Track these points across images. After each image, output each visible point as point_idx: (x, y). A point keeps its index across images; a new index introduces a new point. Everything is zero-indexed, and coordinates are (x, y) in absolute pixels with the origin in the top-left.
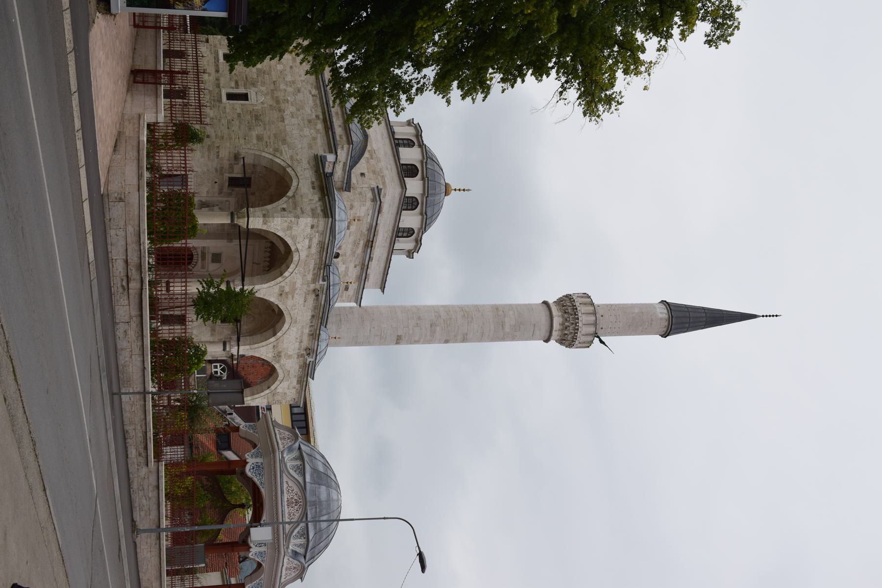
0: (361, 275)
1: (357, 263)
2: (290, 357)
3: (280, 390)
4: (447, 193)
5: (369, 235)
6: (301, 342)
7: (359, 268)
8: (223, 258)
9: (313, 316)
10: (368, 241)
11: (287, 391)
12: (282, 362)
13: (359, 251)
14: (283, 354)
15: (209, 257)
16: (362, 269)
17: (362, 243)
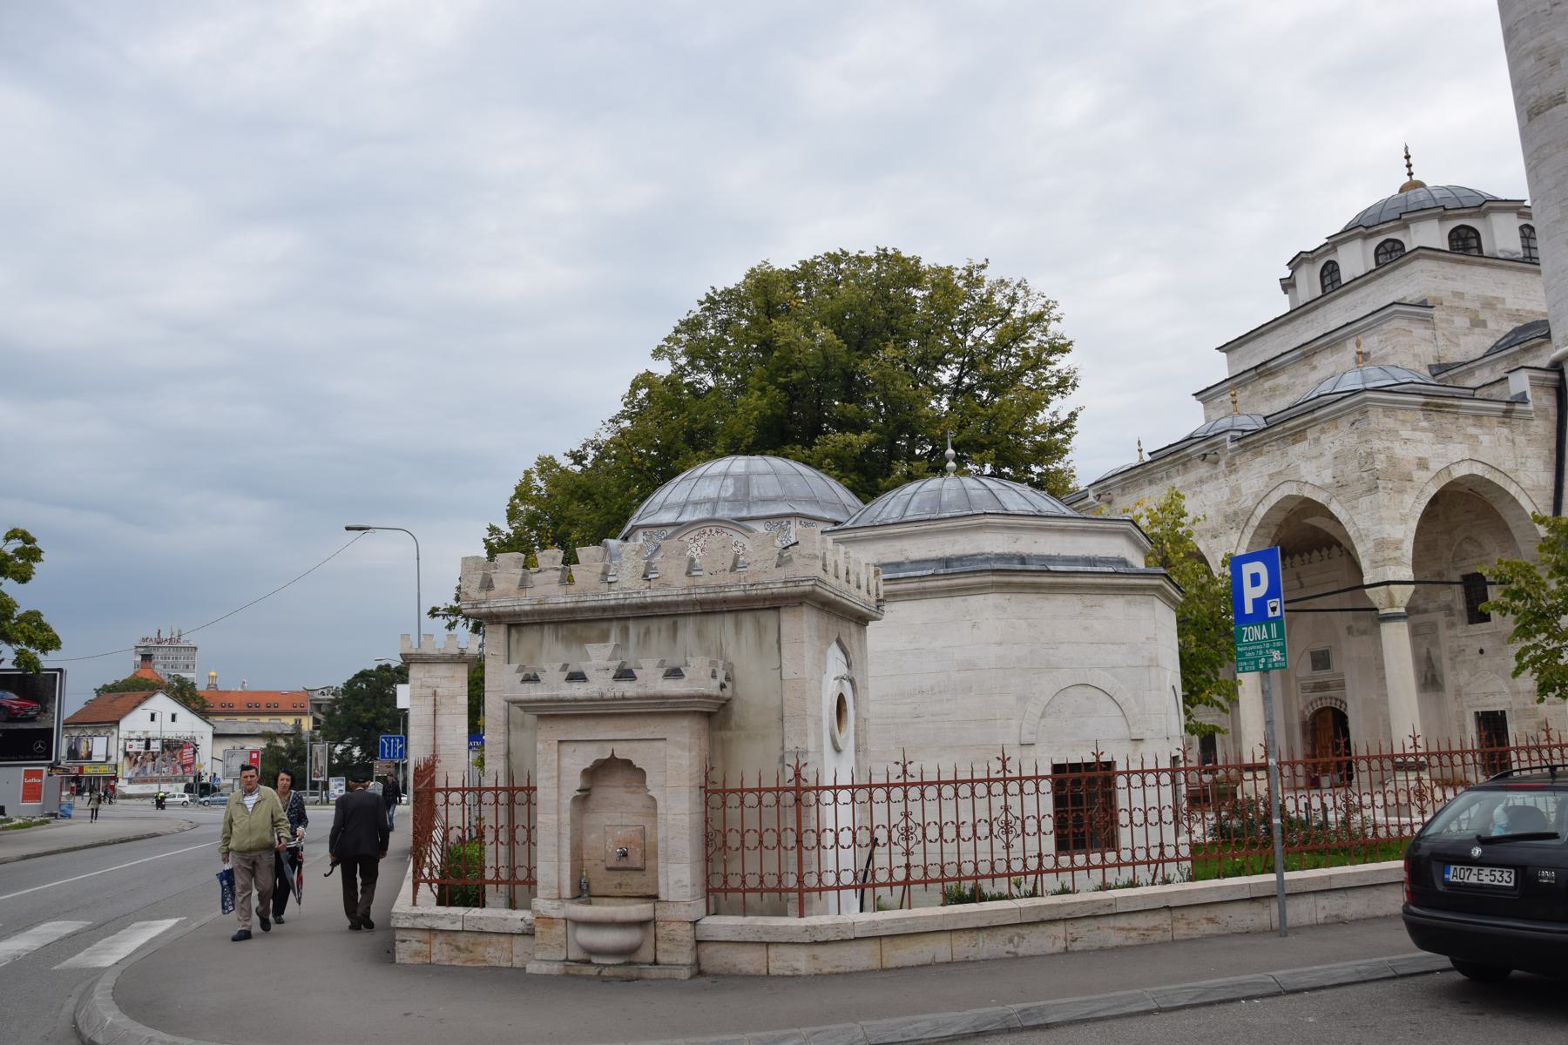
0: (1328, 346)
1: (1305, 369)
2: (1235, 491)
3: (1327, 477)
4: (1420, 184)
5: (1252, 380)
6: (1201, 481)
7: (1316, 360)
8: (1320, 646)
9: (1151, 482)
10: (1260, 375)
11: (1329, 456)
12: (1250, 503)
13: (1282, 379)
14: (1230, 510)
15: (1322, 675)
16: (1315, 352)
17: (1268, 384)
